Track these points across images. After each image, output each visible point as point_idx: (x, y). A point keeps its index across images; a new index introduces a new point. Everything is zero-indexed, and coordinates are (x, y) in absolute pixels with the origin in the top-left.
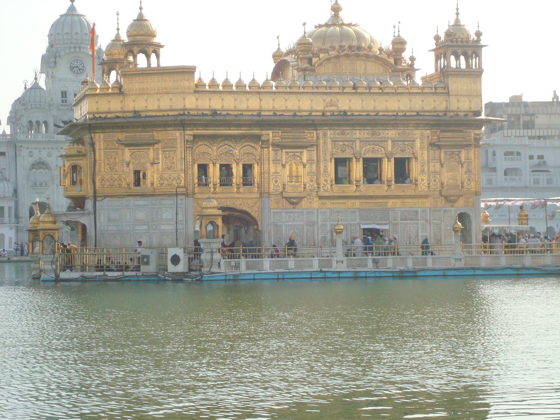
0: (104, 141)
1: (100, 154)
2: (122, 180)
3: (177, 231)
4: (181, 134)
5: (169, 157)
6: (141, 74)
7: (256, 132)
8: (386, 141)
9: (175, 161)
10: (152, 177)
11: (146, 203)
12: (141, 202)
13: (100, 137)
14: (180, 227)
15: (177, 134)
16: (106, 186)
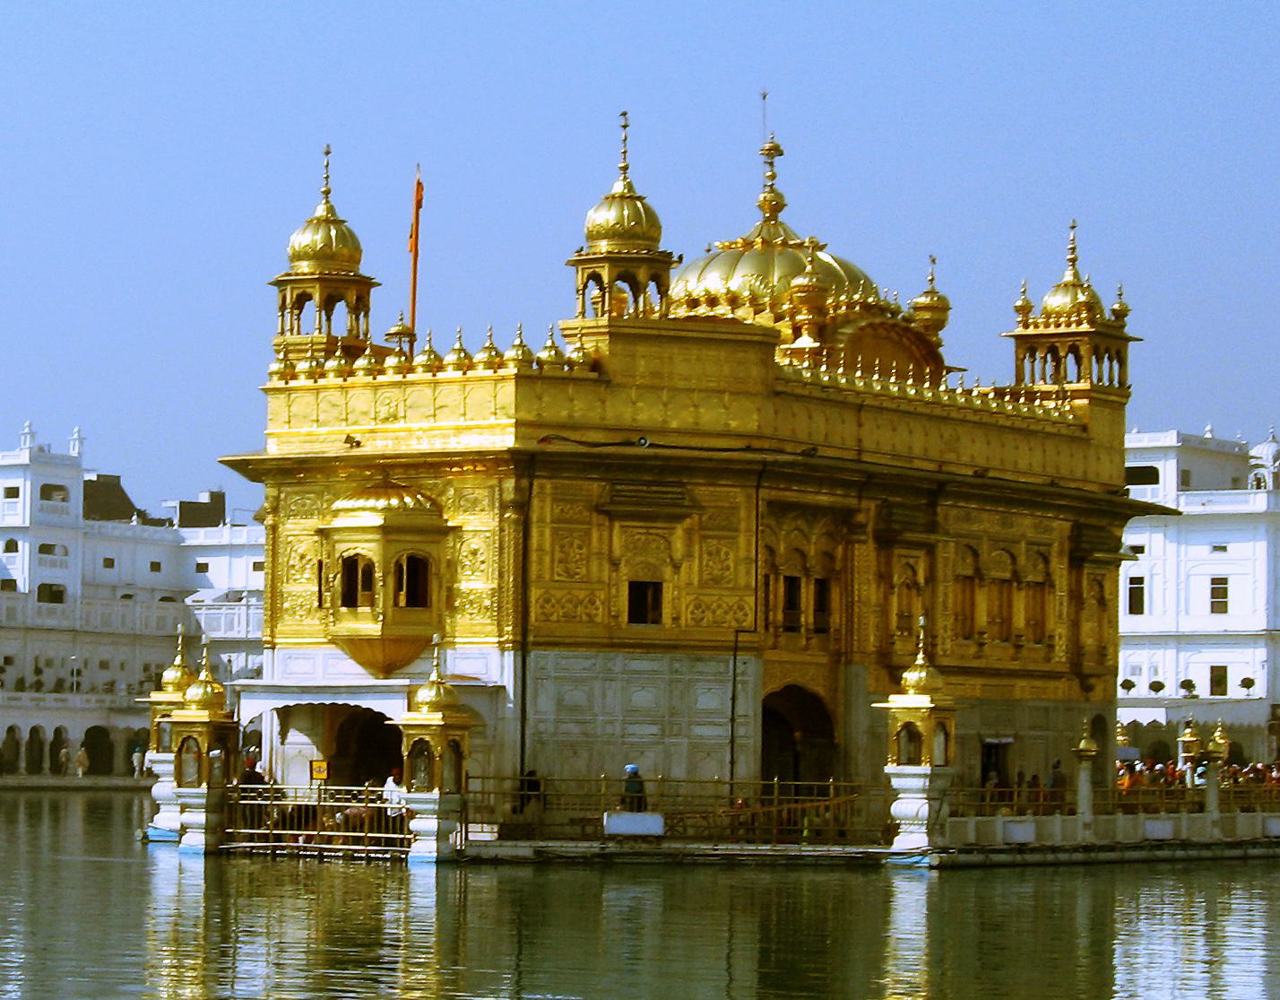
0: (555, 500)
1: (542, 535)
2: (598, 603)
3: (732, 742)
4: (749, 497)
5: (718, 552)
6: (658, 337)
7: (852, 502)
8: (1018, 542)
9: (731, 563)
10: (675, 601)
11: (654, 666)
12: (642, 664)
13: (542, 487)
14: (741, 731)
15: (738, 495)
16: (554, 618)
